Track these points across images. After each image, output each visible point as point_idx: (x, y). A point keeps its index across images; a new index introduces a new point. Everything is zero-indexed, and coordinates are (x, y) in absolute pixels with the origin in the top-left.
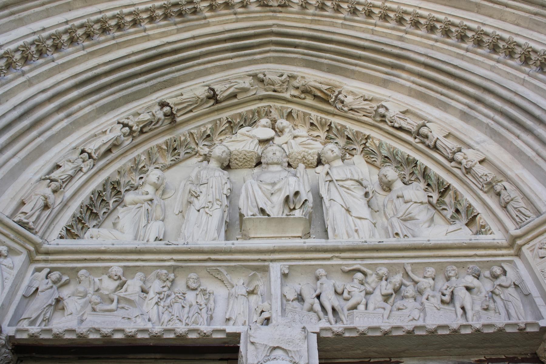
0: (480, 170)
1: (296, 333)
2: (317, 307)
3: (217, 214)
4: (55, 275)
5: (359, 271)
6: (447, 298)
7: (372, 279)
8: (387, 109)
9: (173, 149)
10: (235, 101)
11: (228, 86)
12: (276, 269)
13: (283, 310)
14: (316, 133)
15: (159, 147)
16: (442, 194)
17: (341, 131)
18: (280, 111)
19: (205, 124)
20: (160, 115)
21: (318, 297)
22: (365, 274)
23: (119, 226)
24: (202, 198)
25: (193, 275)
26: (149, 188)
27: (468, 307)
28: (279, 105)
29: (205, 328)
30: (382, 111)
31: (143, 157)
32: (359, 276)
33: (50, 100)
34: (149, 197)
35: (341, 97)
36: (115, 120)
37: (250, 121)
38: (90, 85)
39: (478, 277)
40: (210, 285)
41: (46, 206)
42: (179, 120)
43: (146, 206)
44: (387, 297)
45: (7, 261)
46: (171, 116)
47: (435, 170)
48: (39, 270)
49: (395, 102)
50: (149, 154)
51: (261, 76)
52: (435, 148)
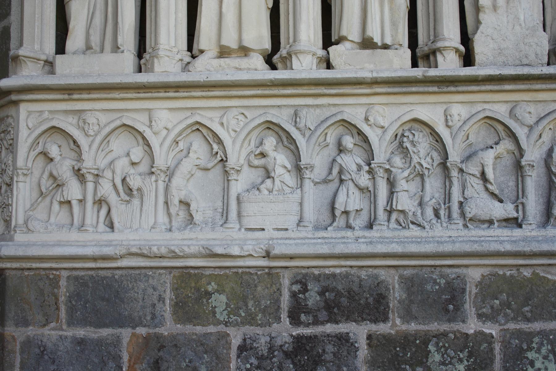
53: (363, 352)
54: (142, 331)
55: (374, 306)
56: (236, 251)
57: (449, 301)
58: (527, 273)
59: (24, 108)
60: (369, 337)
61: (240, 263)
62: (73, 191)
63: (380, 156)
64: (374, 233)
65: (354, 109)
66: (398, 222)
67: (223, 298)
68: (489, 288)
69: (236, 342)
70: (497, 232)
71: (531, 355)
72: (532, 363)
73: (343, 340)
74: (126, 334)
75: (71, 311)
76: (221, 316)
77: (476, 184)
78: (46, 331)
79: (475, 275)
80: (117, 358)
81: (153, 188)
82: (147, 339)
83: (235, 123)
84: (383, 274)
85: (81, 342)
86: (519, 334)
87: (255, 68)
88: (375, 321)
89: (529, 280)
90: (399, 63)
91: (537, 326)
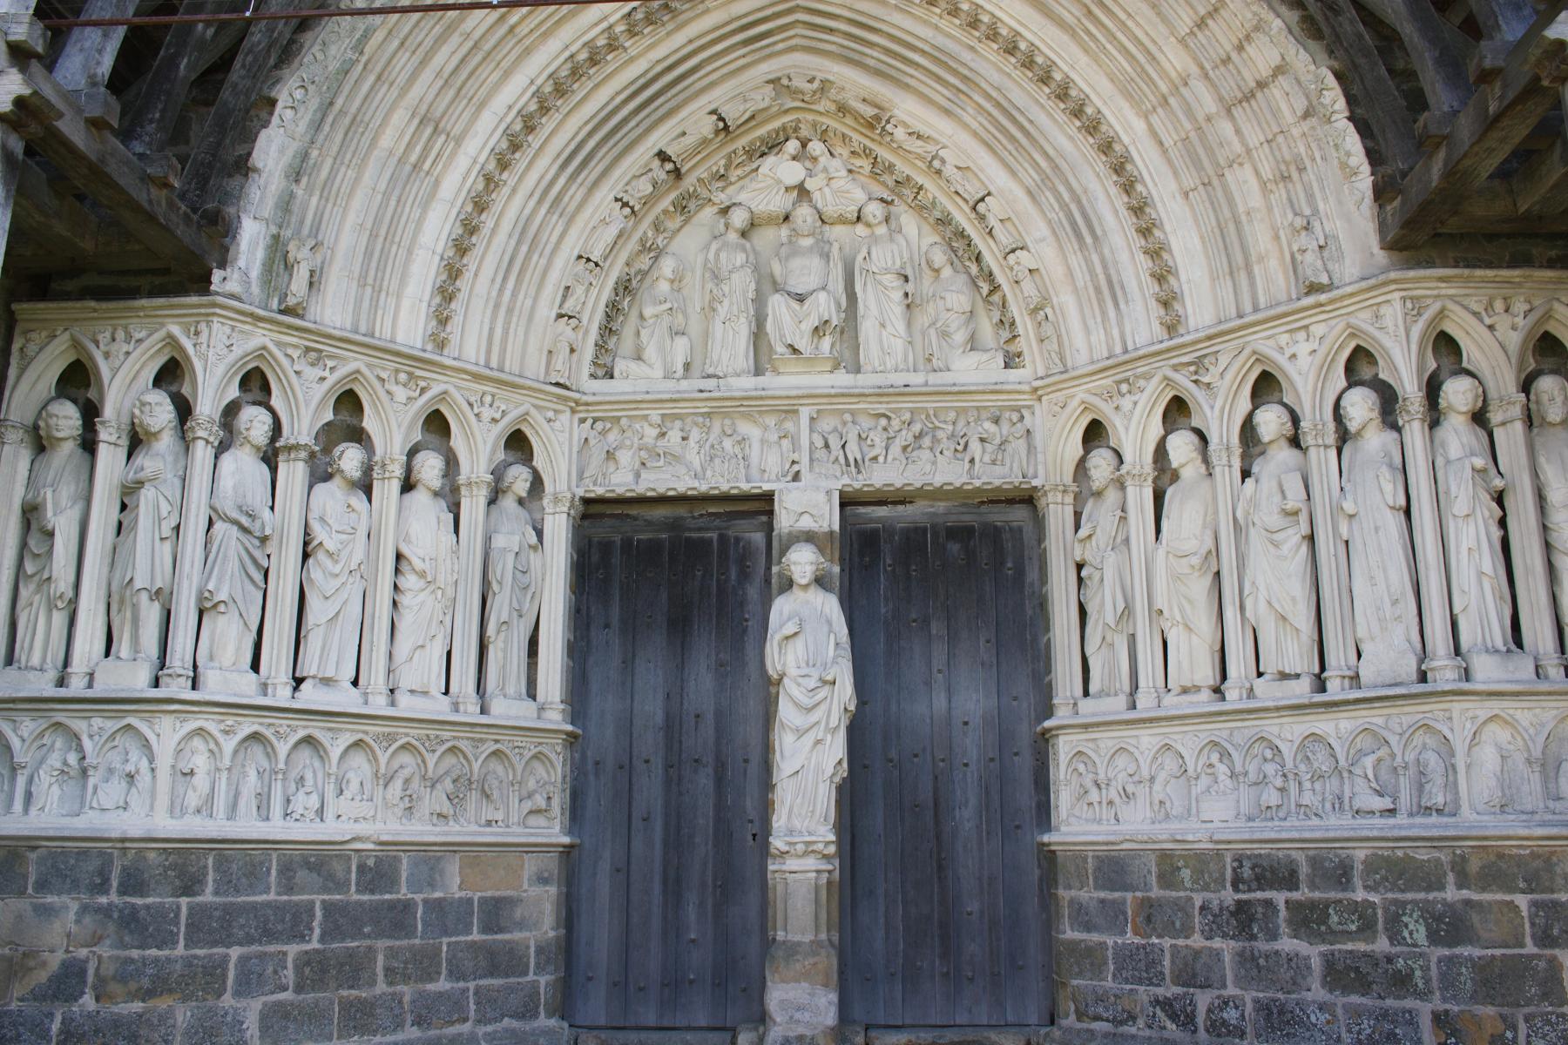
0: (1028, 286)
1: (821, 497)
2: (842, 460)
3: (744, 329)
4: (599, 426)
5: (884, 415)
6: (960, 448)
7: (896, 423)
8: (943, 161)
9: (681, 207)
10: (753, 123)
11: (742, 108)
12: (805, 413)
13: (811, 460)
14: (858, 162)
15: (665, 212)
16: (991, 292)
17: (890, 168)
18: (814, 125)
19: (718, 162)
20: (663, 176)
21: (843, 447)
22: (889, 418)
23: (646, 356)
24: (726, 302)
25: (728, 422)
26: (664, 286)
27: (977, 460)
28: (810, 117)
29: (745, 487)
30: (936, 164)
31: (650, 234)
32: (883, 422)
33: (540, 202)
34: (668, 305)
35: (889, 127)
36: (611, 197)
37: (772, 145)
38: (577, 161)
39: (996, 421)
40: (745, 428)
41: (572, 351)
42: (683, 170)
43: (666, 319)
44: (905, 448)
45: (557, 425)
46: (677, 174)
47: (988, 258)
48: (583, 421)
49: (956, 141)
50: (657, 227)
51: (785, 82)
52: (990, 233)
53: (1283, 913)
54: (1139, 894)
55: (1285, 876)
56: (1190, 838)
57: (1343, 875)
58: (1400, 853)
59: (1061, 739)
60: (1287, 902)
61: (1196, 846)
62: (1094, 795)
63: (1289, 764)
64: (1287, 824)
65: (1271, 727)
66: (1305, 814)
67: (1188, 871)
68: (1371, 865)
69: (1198, 904)
70: (1378, 821)
71: (1405, 919)
72: (1406, 926)
73: (1268, 903)
74: (1129, 896)
75: (1096, 879)
76: (1188, 884)
77: (1360, 781)
78: (1082, 893)
79: (1360, 854)
80: (1125, 913)
81: (1141, 791)
82: (1143, 899)
83: (1189, 741)
84: (1293, 853)
85: (1102, 901)
86: (1395, 902)
87: (1203, 701)
88: (1290, 890)
89: (1402, 859)
90: (1301, 690)
91: (1409, 896)
